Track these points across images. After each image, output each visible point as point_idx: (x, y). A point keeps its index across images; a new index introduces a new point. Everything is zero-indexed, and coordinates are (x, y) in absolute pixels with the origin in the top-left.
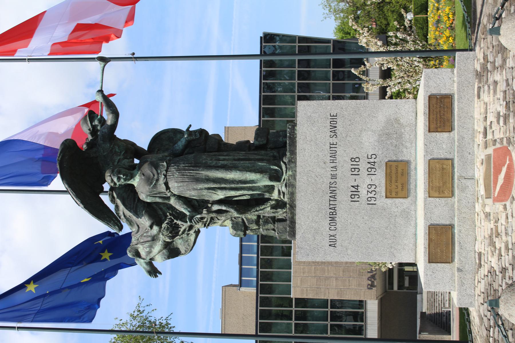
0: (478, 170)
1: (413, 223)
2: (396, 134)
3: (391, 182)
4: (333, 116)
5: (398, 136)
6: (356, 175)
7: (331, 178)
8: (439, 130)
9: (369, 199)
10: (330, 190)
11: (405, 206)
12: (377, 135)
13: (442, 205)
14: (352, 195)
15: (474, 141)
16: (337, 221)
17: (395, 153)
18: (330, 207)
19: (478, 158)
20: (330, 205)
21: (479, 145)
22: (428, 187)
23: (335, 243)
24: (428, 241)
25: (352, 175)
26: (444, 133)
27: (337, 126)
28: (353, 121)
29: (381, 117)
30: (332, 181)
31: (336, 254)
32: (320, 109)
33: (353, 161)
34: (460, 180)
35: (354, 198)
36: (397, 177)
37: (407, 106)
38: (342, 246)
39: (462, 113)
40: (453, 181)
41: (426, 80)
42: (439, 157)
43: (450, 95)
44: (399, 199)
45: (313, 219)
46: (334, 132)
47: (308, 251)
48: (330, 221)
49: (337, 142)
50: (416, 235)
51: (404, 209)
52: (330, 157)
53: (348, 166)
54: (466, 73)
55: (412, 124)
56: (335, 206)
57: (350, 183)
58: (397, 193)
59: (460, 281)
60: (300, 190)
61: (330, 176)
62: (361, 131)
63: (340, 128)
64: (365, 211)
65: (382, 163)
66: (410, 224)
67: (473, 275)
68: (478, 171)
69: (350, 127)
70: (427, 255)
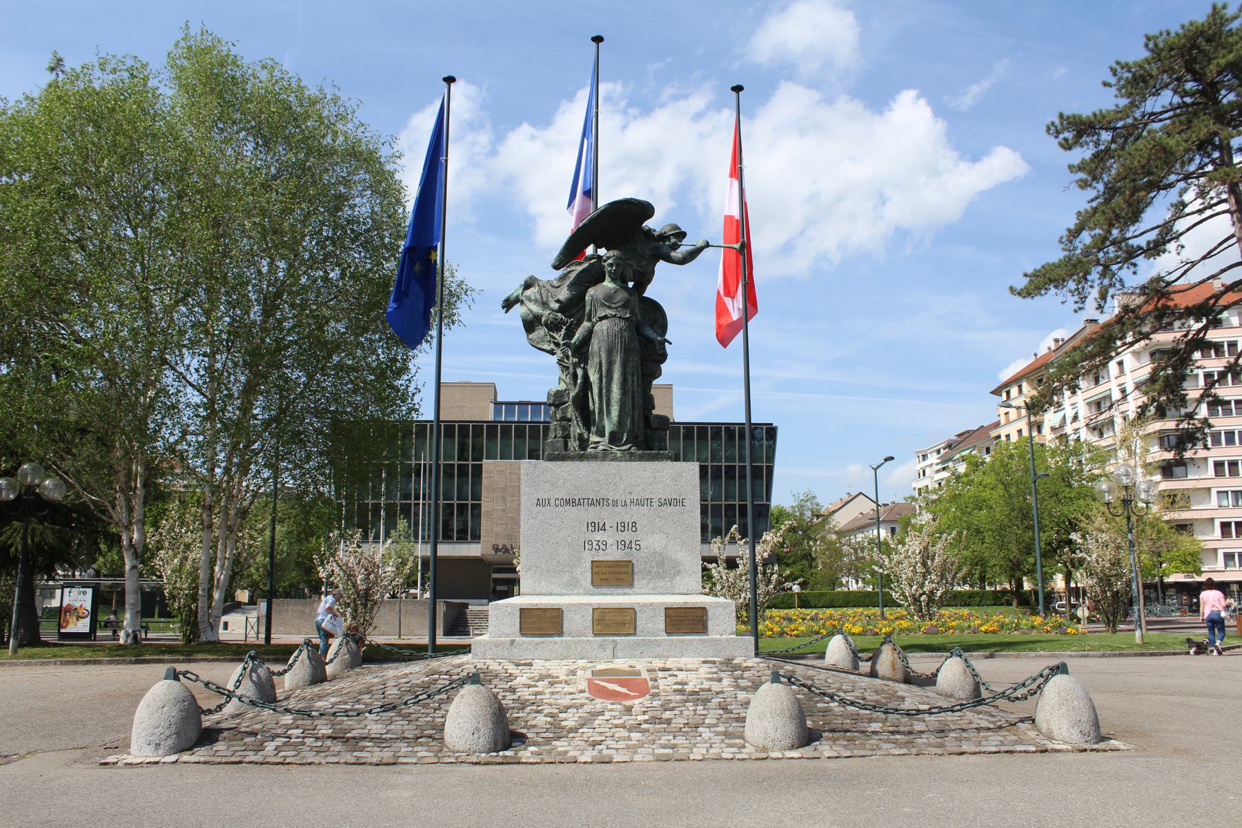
1: (564, 591)
11: (582, 582)
30: (610, 502)
36: (615, 573)
37: (694, 583)
41: (722, 604)
58: (598, 573)
63: (669, 509)
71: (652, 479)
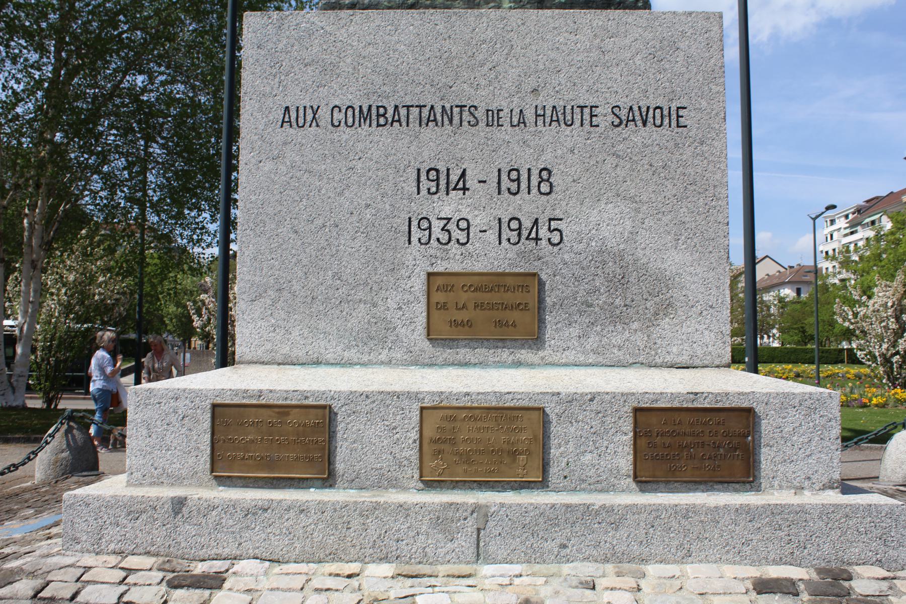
0: (506, 581)
2: (625, 306)
3: (476, 290)
4: (678, 116)
5: (618, 312)
6: (499, 183)
7: (488, 111)
8: (643, 442)
9: (425, 224)
10: (452, 107)
12: (622, 247)
13: (396, 449)
14: (437, 171)
15: (606, 560)
16: (360, 129)
17: (566, 302)
18: (400, 106)
19: (546, 582)
20: (408, 107)
21: (594, 588)
22: (455, 404)
23: (294, 124)
24: (280, 402)
25: (499, 170)
26: (631, 457)
27: (647, 128)
28: (662, 175)
29: (676, 261)
30: (481, 114)
31: (261, 127)
32: (700, 77)
33: (540, 177)
34: (473, 512)
35: (428, 179)
36: (492, 307)
37: (709, 337)
38: (285, 144)
39: (702, 522)
40: (475, 485)
41: (803, 399)
42: (554, 442)
43: (755, 477)
44: (425, 314)
45: (364, 57)
46: (631, 118)
47: (270, 45)
48: (361, 107)
49: (598, 126)
50: (317, 363)
51: (395, 328)
52: (554, 107)
53: (526, 160)
54: (834, 535)
55: (657, 354)
56: (404, 124)
57: (473, 166)
58: (444, 307)
59: (143, 506)
60: (454, 18)
61: (494, 107)
62: (632, 199)
63: (639, 136)
64: (388, 212)
65: (536, 263)
66: (349, 347)
67: (162, 549)
68: (501, 580)
69: (646, 167)
70: (236, 401)
71: (594, 54)
